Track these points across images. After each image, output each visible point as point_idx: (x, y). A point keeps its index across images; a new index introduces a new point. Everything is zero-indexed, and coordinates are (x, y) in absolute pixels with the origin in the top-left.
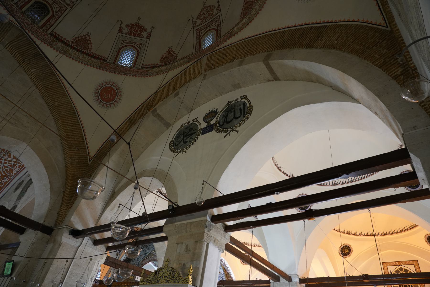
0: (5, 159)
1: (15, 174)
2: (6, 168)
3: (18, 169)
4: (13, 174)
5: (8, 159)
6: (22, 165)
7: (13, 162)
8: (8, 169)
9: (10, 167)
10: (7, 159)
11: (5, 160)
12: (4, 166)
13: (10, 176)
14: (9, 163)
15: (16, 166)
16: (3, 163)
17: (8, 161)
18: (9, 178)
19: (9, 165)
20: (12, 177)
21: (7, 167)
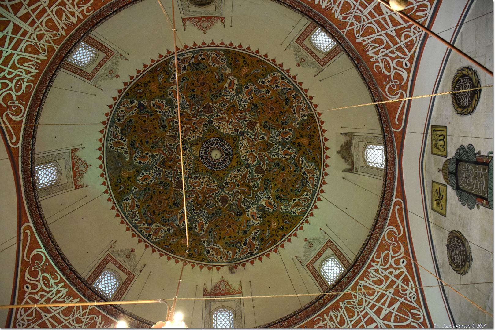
0: (369, 306)
1: (418, 301)
2: (391, 317)
3: (410, 291)
4: (414, 308)
5: (372, 300)
6: (406, 273)
7: (388, 293)
8: (396, 315)
9: (397, 305)
10: (373, 302)
11: (371, 308)
12: (384, 319)
13: (415, 317)
14: (383, 304)
15: (400, 287)
16: (375, 317)
17: (378, 301)
18: (418, 325)
19: (389, 306)
20: (422, 313)
21: (391, 313)
